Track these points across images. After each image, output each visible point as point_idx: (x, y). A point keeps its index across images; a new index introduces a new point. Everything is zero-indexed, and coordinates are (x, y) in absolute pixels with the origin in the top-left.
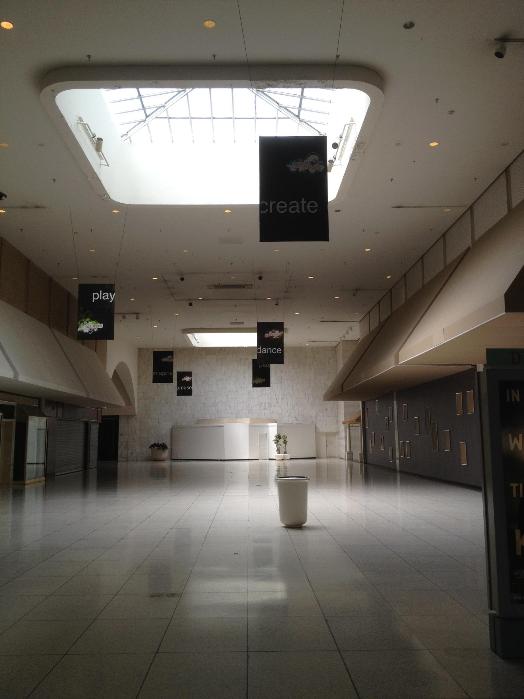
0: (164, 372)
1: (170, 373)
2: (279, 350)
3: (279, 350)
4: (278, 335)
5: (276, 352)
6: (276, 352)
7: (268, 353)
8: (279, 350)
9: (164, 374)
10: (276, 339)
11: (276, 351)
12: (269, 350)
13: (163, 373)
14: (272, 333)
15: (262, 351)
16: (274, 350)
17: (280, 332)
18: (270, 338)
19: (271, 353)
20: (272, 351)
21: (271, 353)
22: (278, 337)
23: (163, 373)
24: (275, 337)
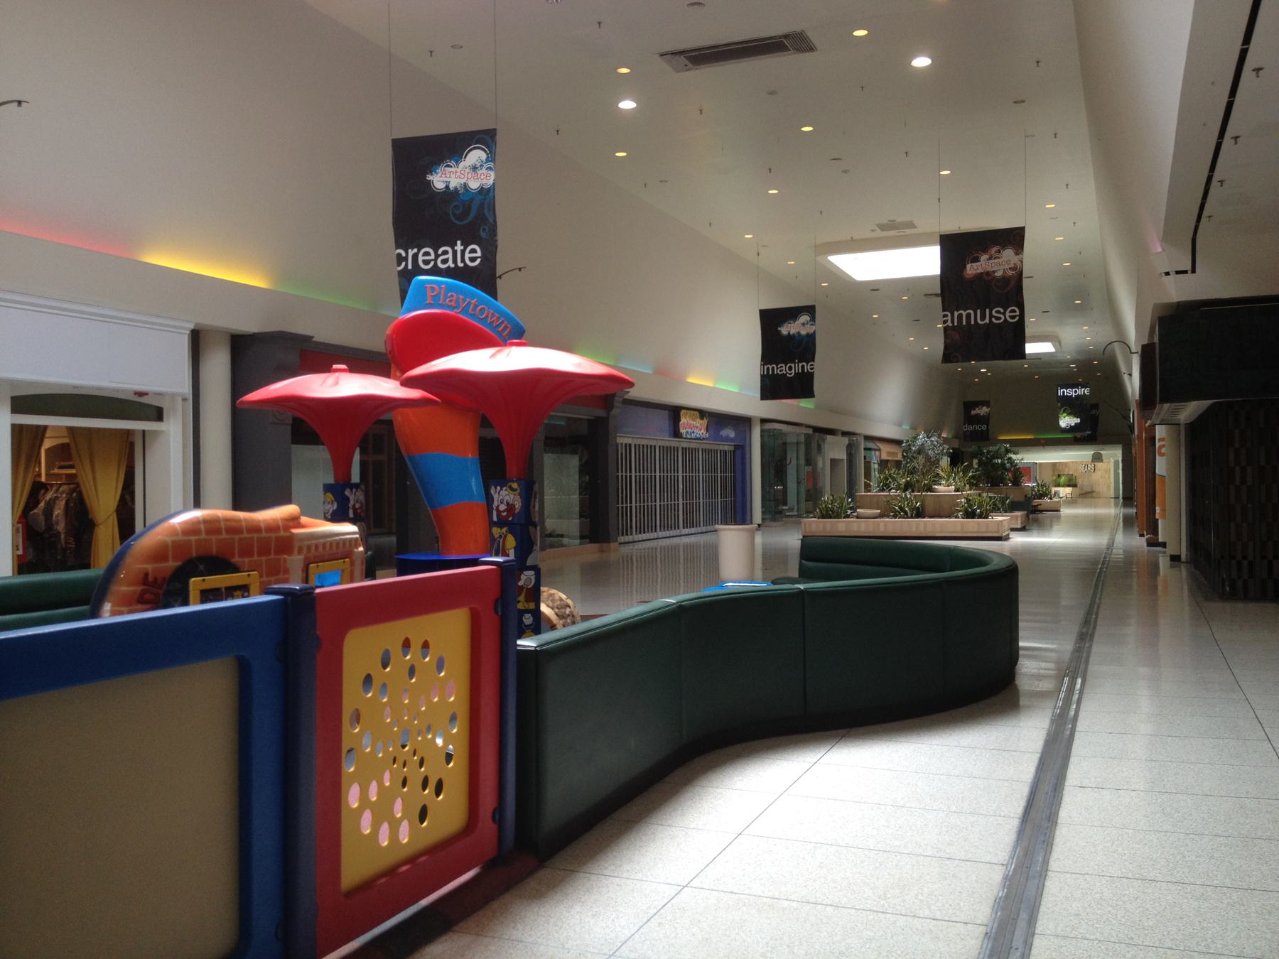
0: (793, 365)
1: (808, 368)
4: (1012, 266)
9: (793, 371)
13: (790, 368)
14: (990, 258)
18: (984, 279)
22: (1010, 273)
23: (790, 368)
24: (999, 274)
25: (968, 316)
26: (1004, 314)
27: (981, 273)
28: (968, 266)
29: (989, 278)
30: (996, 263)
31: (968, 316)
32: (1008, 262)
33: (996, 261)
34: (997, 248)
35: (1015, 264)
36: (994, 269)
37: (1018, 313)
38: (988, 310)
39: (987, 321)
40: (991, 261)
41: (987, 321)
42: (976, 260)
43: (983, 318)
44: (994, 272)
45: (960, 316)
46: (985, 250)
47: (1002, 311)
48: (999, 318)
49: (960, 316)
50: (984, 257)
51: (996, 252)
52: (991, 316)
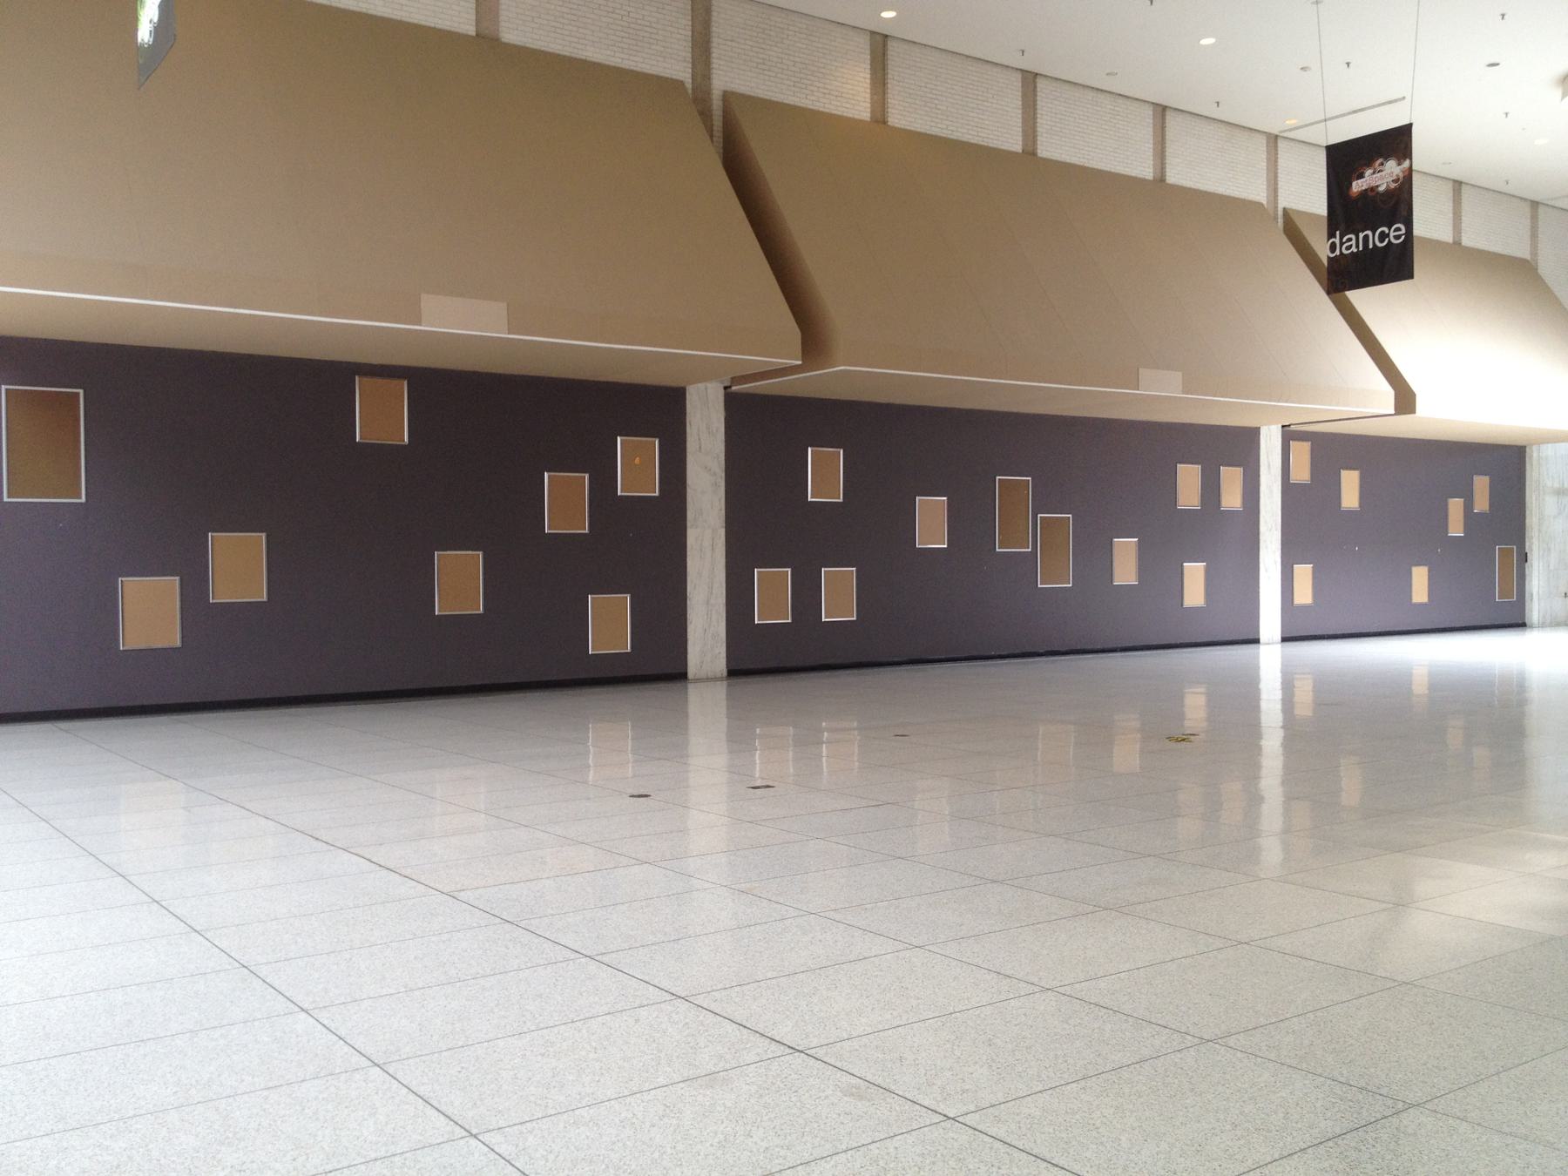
2: (1395, 230)
3: (1398, 229)
5: (1387, 240)
6: (1387, 240)
7: (1361, 249)
8: (1395, 230)
10: (1389, 193)
11: (1388, 235)
12: (1366, 237)
14: (1374, 173)
15: (1344, 246)
16: (1383, 232)
17: (1399, 165)
18: (1370, 194)
19: (1371, 247)
20: (1374, 240)
21: (1371, 247)
22: (1393, 186)
24: (1382, 189)
27: (1366, 190)
28: (1354, 184)
29: (1373, 194)
30: (1380, 177)
33: (1380, 173)
40: (1374, 176)
42: (1361, 176)
44: (1377, 186)
46: (1369, 164)
50: (1368, 172)
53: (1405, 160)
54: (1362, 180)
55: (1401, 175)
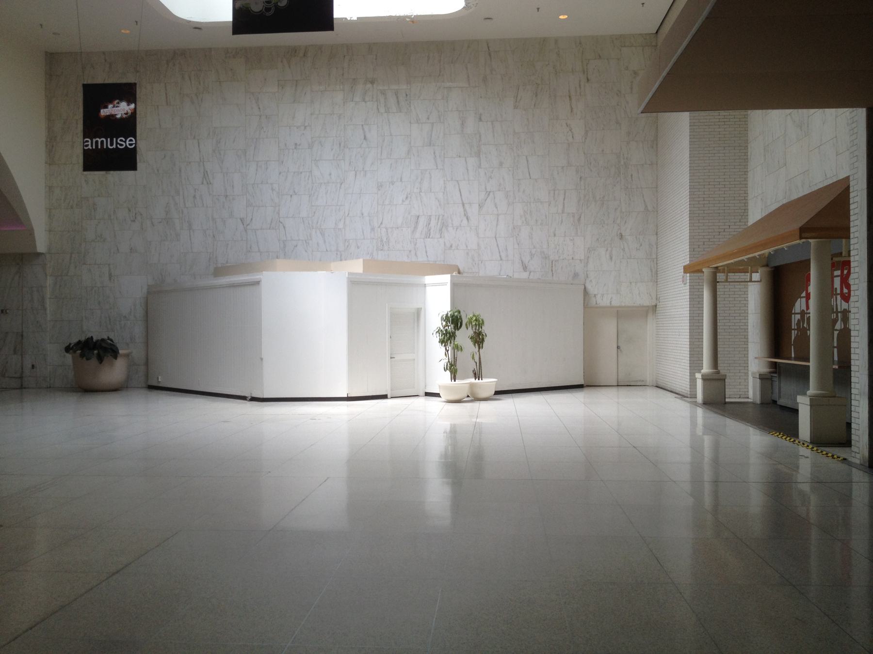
3: (131, 140)
14: (114, 107)
18: (111, 118)
22: (124, 116)
24: (118, 116)
25: (102, 142)
26: (125, 142)
31: (102, 142)
32: (124, 110)
33: (117, 108)
34: (117, 101)
35: (127, 111)
36: (116, 113)
37: (134, 142)
38: (115, 139)
39: (114, 146)
40: (114, 109)
41: (114, 146)
42: (106, 107)
43: (112, 144)
44: (116, 115)
45: (97, 142)
46: (111, 102)
47: (124, 140)
48: (121, 145)
49: (97, 142)
50: (110, 106)
51: (117, 103)
52: (117, 143)
53: (132, 103)
54: (107, 109)
55: (130, 112)
